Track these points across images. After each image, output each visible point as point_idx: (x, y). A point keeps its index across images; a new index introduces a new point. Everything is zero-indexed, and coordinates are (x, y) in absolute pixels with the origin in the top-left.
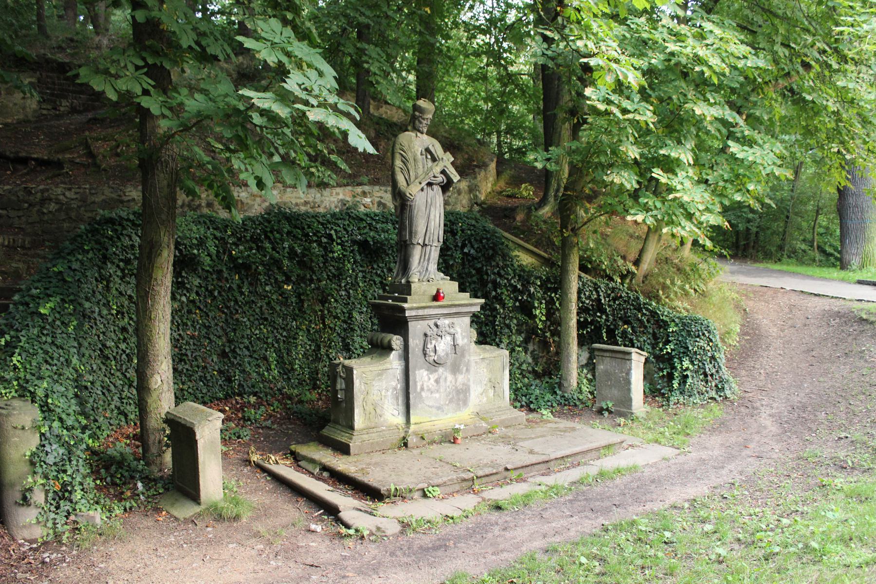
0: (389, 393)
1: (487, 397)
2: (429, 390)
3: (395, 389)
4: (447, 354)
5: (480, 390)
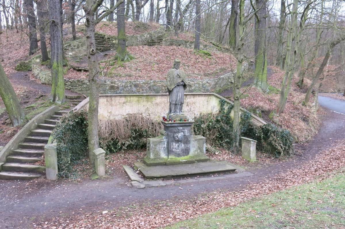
0: (162, 149)
1: (197, 152)
2: (175, 148)
4: (181, 138)
5: (195, 149)
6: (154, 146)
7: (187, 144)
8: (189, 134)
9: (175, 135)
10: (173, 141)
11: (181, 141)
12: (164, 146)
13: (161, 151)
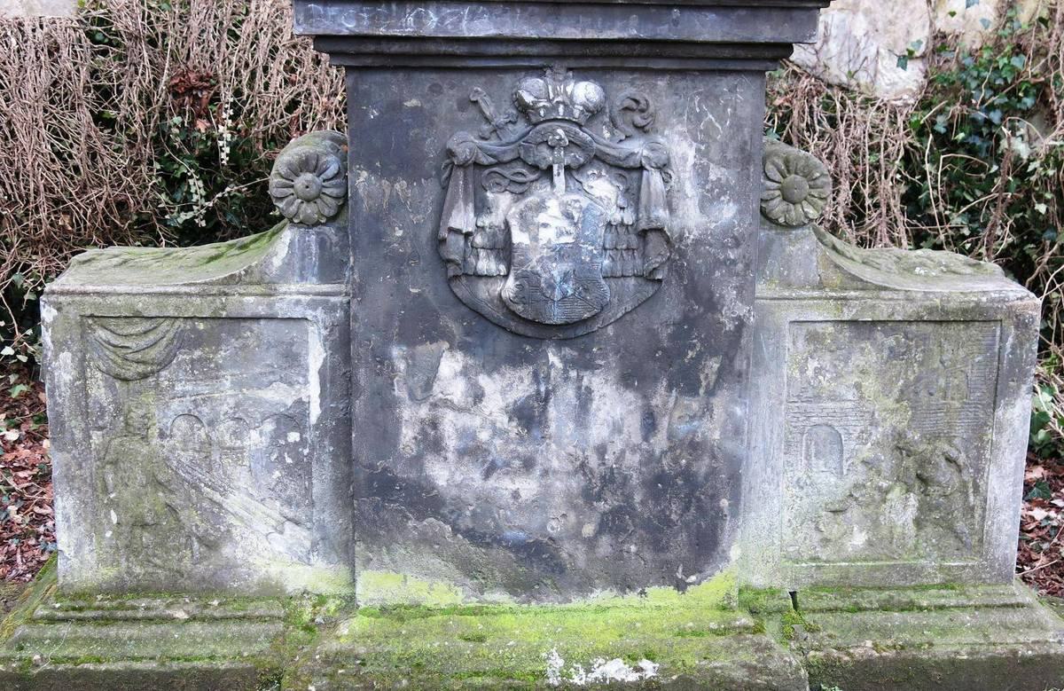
0: (256, 439)
2: (472, 451)
3: (293, 418)
4: (584, 280)
5: (829, 481)
6: (99, 391)
7: (687, 382)
8: (727, 212)
9: (462, 218)
10: (420, 327)
11: (573, 334)
12: (278, 395)
13: (241, 477)
